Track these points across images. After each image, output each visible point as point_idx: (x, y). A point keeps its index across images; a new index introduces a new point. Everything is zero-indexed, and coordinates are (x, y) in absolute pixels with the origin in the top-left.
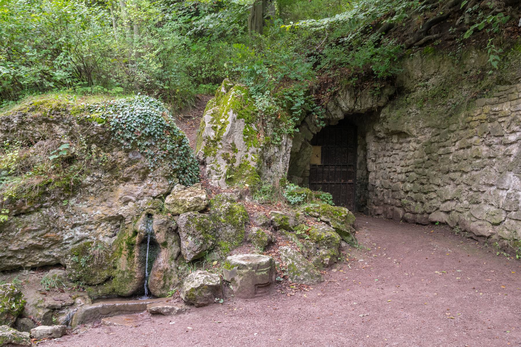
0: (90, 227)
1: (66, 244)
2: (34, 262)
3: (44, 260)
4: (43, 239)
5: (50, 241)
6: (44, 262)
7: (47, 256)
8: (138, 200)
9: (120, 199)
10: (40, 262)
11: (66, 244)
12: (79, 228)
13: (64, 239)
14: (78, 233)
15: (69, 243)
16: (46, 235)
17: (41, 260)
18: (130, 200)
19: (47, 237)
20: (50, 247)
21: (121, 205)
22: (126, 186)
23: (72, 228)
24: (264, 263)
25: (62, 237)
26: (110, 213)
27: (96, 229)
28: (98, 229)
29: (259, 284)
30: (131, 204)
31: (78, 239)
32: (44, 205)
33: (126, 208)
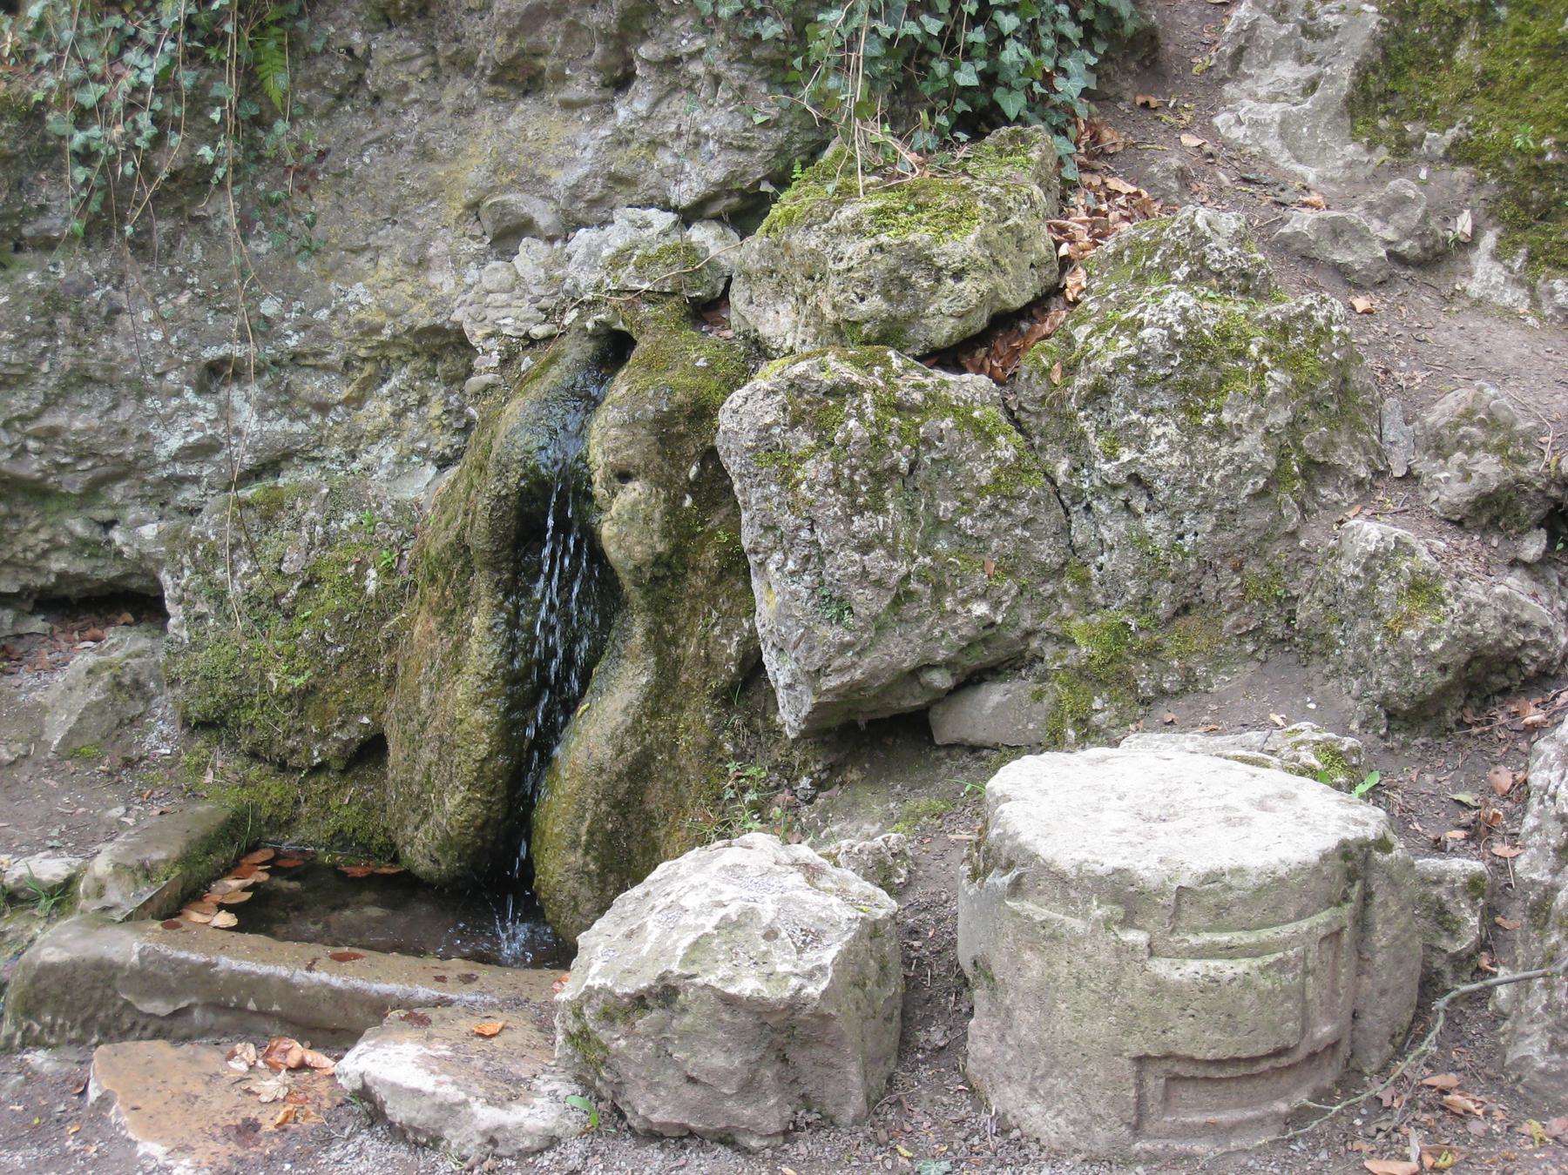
0: (313, 385)
1: (180, 481)
2: (36, 570)
3: (81, 566)
4: (32, 444)
5: (81, 458)
6: (80, 578)
7: (82, 546)
8: (570, 224)
9: (474, 206)
10: (61, 576)
11: (180, 481)
12: (254, 389)
13: (162, 454)
14: (247, 419)
15: (196, 480)
16: (48, 421)
17: (58, 564)
18: (525, 227)
19: (54, 432)
20: (94, 490)
21: (481, 260)
22: (513, 122)
23: (201, 389)
24: (1251, 881)
25: (144, 437)
26: (419, 308)
27: (355, 402)
28: (370, 406)
29: (1168, 1057)
30: (530, 257)
31: (248, 460)
32: (27, 231)
33: (496, 273)
